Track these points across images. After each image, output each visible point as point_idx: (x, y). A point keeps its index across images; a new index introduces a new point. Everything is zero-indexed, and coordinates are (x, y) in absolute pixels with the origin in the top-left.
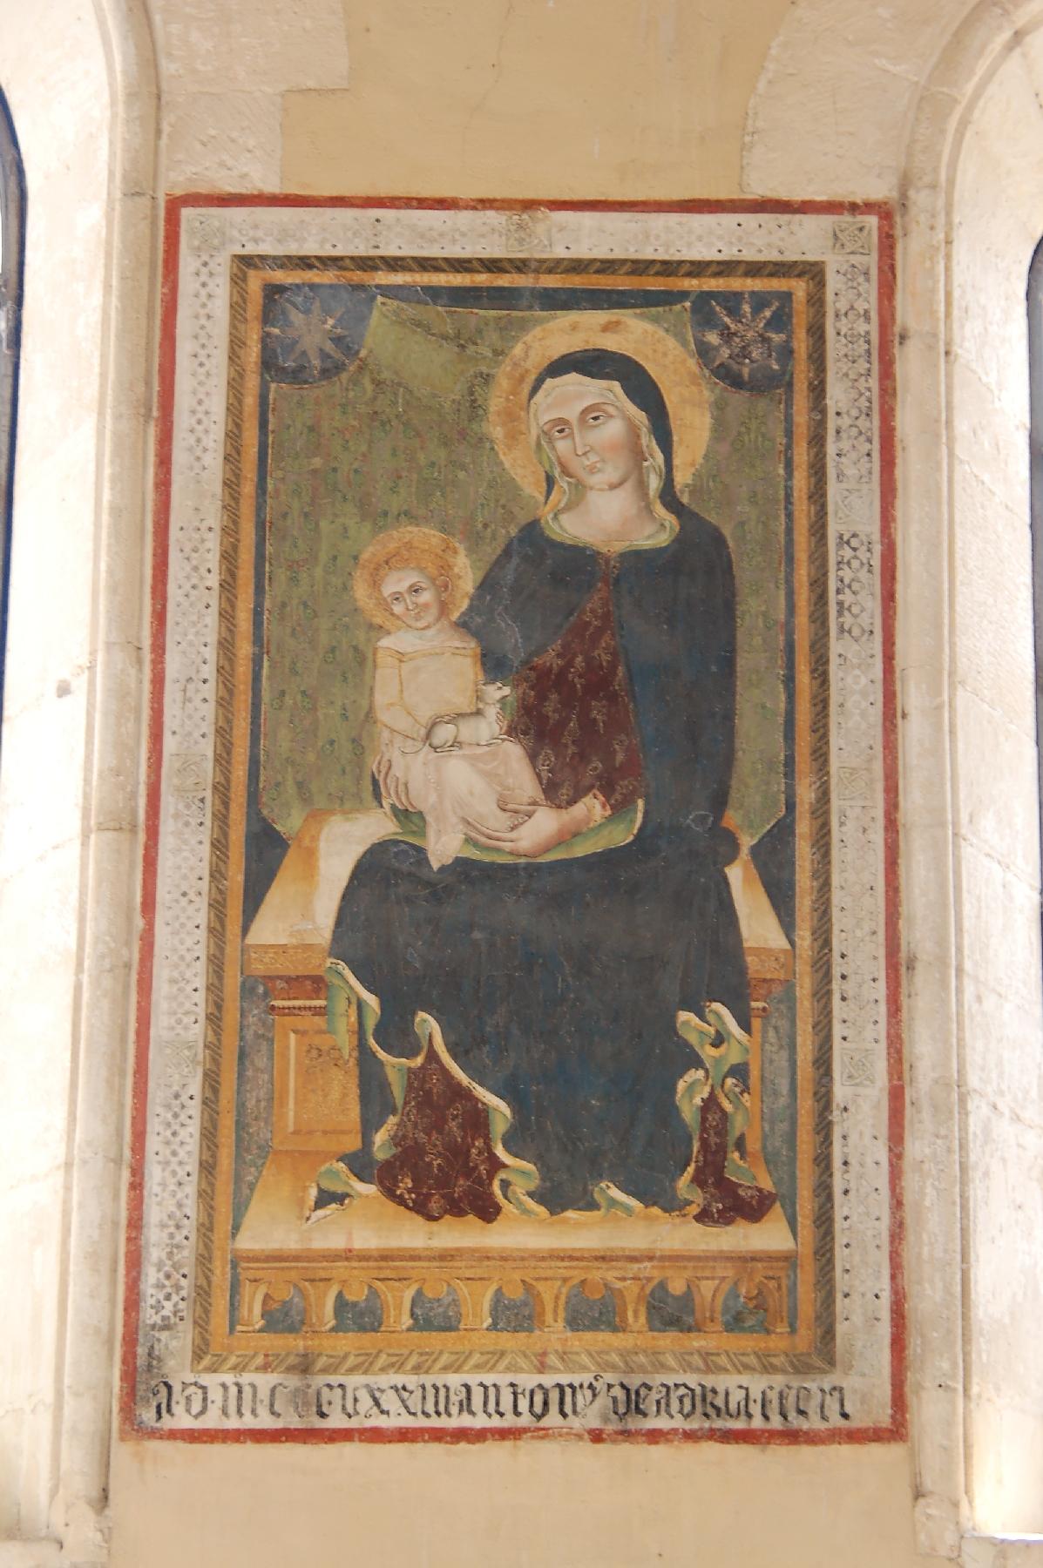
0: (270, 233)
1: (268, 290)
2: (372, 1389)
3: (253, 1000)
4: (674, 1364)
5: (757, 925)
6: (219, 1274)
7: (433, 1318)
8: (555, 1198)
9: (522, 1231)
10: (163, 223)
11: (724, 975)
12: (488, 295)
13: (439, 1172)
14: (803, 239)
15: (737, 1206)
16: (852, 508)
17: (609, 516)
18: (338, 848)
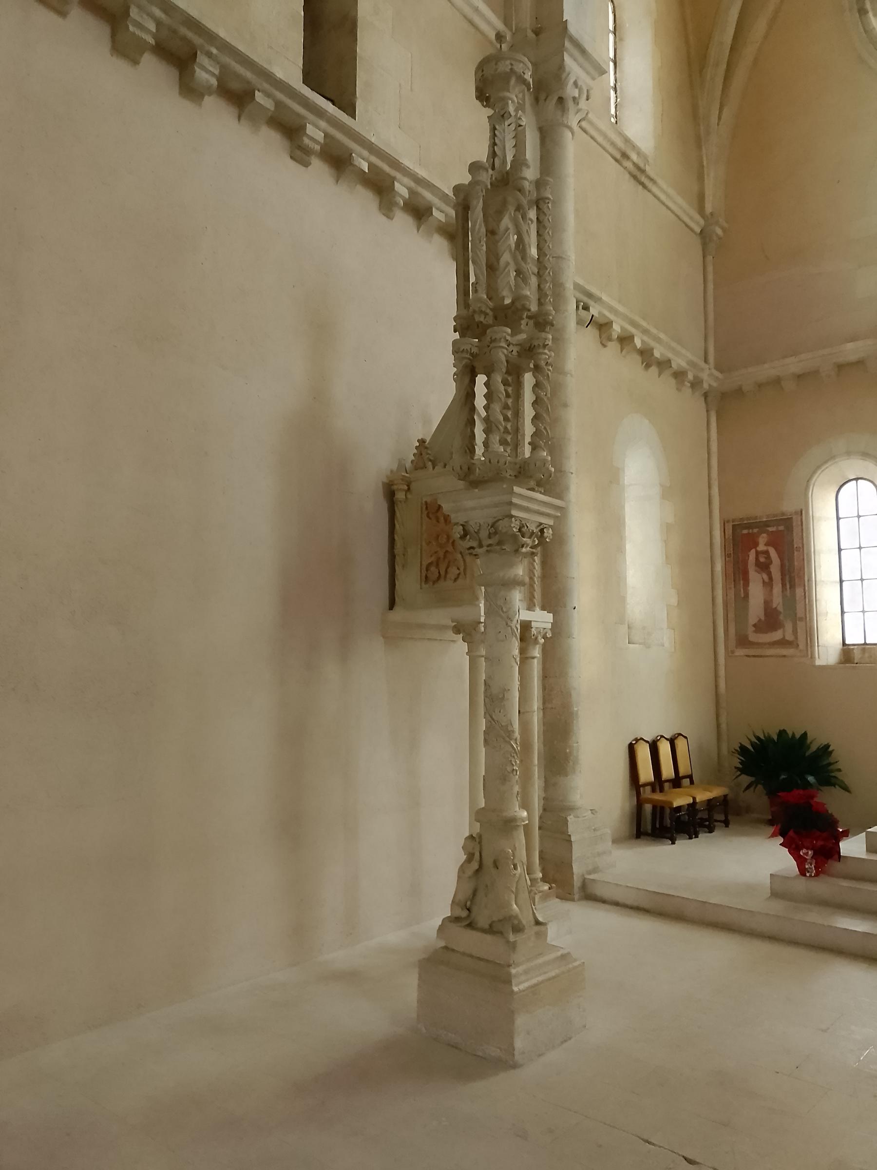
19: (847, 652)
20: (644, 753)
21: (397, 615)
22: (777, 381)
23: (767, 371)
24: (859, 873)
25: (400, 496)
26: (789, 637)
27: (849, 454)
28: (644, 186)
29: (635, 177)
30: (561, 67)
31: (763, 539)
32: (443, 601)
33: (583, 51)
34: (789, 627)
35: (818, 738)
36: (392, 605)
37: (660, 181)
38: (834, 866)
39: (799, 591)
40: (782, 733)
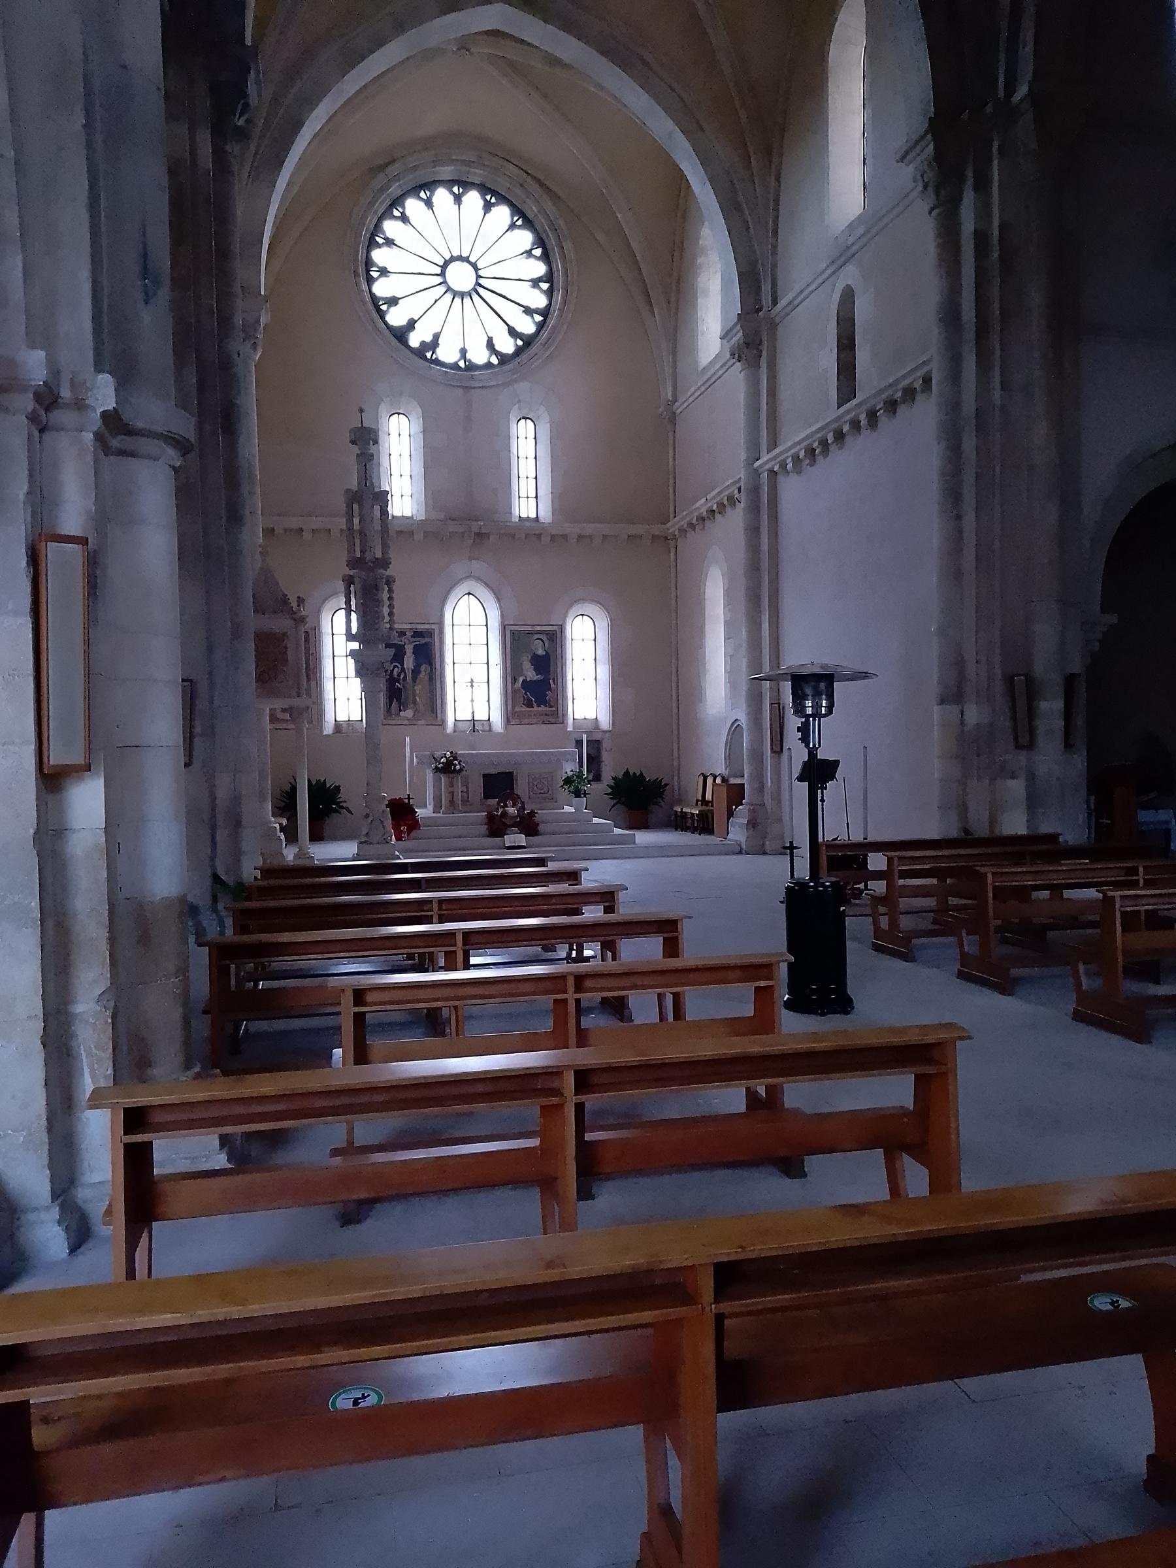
1: (513, 633)
3: (514, 691)
4: (546, 718)
5: (552, 685)
6: (513, 712)
7: (530, 715)
8: (539, 706)
10: (504, 627)
11: (550, 689)
12: (531, 633)
13: (530, 705)
14: (555, 628)
16: (559, 651)
17: (540, 652)
18: (521, 679)
19: (338, 726)
23: (294, 523)
38: (414, 834)
39: (313, 684)
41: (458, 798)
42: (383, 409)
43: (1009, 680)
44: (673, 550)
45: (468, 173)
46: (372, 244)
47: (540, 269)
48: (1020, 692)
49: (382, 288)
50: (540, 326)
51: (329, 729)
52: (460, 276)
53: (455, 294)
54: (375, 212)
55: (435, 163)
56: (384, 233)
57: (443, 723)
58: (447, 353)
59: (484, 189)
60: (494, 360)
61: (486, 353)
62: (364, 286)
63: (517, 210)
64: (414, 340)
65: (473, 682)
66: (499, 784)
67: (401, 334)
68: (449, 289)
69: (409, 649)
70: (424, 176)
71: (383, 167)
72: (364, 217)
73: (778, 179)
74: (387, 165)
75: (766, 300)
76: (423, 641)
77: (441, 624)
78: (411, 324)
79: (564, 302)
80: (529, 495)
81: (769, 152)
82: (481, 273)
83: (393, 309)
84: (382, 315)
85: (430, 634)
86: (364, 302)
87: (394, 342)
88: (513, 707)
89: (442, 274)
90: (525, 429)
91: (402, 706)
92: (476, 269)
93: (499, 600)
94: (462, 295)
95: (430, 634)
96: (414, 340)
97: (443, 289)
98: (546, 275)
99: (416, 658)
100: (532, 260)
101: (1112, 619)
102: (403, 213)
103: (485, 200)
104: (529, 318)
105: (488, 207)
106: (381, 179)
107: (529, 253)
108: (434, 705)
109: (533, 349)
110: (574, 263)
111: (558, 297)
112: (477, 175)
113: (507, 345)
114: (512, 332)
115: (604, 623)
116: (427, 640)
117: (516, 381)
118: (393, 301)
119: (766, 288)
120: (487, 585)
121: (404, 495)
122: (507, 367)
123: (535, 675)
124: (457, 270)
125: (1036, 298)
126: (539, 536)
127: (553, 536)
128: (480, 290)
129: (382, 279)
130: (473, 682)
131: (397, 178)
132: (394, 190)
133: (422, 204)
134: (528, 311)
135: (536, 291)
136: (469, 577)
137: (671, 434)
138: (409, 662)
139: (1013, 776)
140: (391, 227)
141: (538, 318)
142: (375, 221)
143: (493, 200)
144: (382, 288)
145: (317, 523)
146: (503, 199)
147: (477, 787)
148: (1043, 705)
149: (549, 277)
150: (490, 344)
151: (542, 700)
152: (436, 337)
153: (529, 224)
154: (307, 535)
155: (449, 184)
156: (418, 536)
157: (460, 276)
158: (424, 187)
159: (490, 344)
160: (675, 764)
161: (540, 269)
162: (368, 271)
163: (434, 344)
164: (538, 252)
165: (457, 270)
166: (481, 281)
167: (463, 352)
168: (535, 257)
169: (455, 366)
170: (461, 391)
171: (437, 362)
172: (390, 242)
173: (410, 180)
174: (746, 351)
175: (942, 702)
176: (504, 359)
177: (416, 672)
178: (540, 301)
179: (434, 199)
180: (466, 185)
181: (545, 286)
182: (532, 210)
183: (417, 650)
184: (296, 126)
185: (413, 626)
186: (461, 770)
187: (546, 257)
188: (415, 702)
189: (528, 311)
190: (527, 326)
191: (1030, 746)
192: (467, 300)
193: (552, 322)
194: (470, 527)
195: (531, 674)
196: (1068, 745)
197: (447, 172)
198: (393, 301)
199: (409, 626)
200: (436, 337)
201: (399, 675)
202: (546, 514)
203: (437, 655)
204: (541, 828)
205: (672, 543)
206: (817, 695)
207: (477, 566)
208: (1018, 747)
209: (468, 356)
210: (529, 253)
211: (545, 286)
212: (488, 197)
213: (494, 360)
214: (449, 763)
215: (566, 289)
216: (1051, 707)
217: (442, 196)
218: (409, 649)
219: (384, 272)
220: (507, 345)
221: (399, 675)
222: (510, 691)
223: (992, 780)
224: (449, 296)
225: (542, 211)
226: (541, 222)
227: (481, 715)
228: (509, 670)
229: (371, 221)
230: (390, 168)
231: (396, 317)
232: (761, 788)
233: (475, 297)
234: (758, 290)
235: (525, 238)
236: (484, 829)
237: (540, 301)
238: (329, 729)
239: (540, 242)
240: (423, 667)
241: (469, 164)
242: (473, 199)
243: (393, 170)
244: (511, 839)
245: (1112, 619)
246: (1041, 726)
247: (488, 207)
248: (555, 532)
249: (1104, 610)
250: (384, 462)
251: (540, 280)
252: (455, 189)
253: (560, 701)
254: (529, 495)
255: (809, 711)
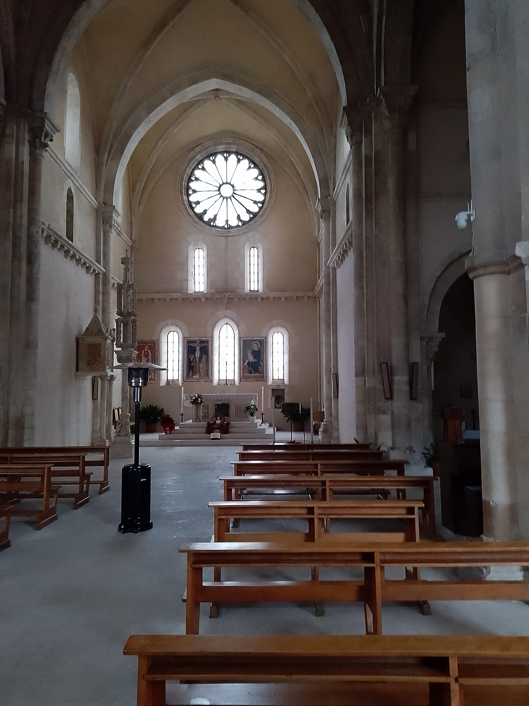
0: (243, 338)
1: (244, 341)
2: (248, 380)
3: (244, 367)
4: (258, 379)
6: (243, 377)
9: (253, 374)
12: (252, 341)
13: (250, 372)
15: (260, 373)
16: (265, 349)
17: (256, 349)
18: (247, 362)
20: (116, 411)
21: (79, 373)
22: (153, 299)
23: (151, 296)
24: (178, 432)
25: (80, 342)
26: (153, 378)
27: (172, 325)
28: (120, 236)
29: (118, 234)
30: (112, 216)
31: (146, 347)
32: (93, 370)
33: (117, 212)
34: (153, 374)
35: (160, 406)
36: (77, 370)
37: (124, 235)
38: (173, 431)
40: (150, 406)
41: (201, 414)
42: (190, 247)
43: (380, 365)
44: (318, 303)
45: (230, 148)
46: (190, 180)
47: (262, 184)
48: (387, 371)
49: (193, 198)
50: (261, 208)
51: (163, 383)
52: (227, 191)
53: (224, 198)
54: (191, 167)
55: (216, 145)
56: (195, 176)
57: (212, 381)
58: (220, 222)
59: (237, 154)
60: (240, 224)
61: (237, 221)
62: (185, 198)
63: (251, 161)
64: (206, 218)
65: (226, 362)
66: (223, 409)
67: (200, 217)
68: (221, 196)
69: (198, 348)
70: (211, 150)
71: (192, 149)
72: (185, 170)
73: (335, 137)
74: (195, 147)
75: (331, 191)
76: (204, 345)
77: (212, 337)
78: (205, 212)
79: (270, 198)
80: (254, 280)
81: (332, 127)
82: (235, 188)
83: (198, 206)
84: (193, 209)
85: (207, 342)
86: (184, 204)
87: (197, 220)
88: (243, 373)
89: (219, 190)
90: (254, 252)
91: (194, 373)
92: (220, 186)
93: (238, 327)
94: (227, 198)
95: (207, 342)
96: (206, 218)
97: (219, 196)
98: (263, 187)
99: (201, 353)
100: (258, 181)
101: (444, 335)
102: (203, 167)
103: (238, 158)
104: (255, 205)
105: (239, 161)
106: (192, 154)
107: (256, 179)
108: (208, 373)
109: (256, 218)
110: (275, 181)
111: (268, 195)
112: (234, 148)
113: (246, 217)
114: (248, 211)
115: (286, 336)
116: (206, 344)
117: (246, 232)
118: (198, 203)
119: (331, 186)
120: (233, 320)
121: (198, 282)
122: (246, 226)
123: (254, 360)
124: (227, 188)
125: (391, 183)
126: (256, 298)
127: (262, 298)
128: (235, 196)
129: (194, 194)
130: (226, 362)
131: (200, 152)
132: (199, 157)
133: (211, 162)
134: (255, 202)
135: (259, 194)
136: (226, 316)
137: (318, 251)
138: (197, 354)
139: (384, 413)
140: (198, 173)
141: (260, 205)
142: (191, 170)
143: (241, 158)
144: (193, 198)
145: (159, 296)
146: (245, 157)
147: (212, 412)
148: (396, 378)
149: (265, 188)
150: (239, 217)
151: (256, 371)
152: (215, 216)
153: (256, 166)
154: (156, 301)
155: (222, 153)
156: (203, 300)
157: (227, 191)
158: (211, 155)
159: (239, 217)
160: (319, 401)
161: (262, 184)
162: (188, 191)
163: (215, 219)
164: (260, 177)
165: (227, 188)
166: (236, 192)
167: (227, 221)
168: (259, 180)
169: (223, 228)
170: (224, 238)
171: (216, 227)
172: (197, 179)
173: (205, 153)
174: (324, 215)
175: (356, 375)
176: (244, 223)
177: (201, 358)
178: (261, 198)
179: (216, 160)
180: (230, 153)
181: (263, 191)
182: (257, 161)
183: (201, 349)
184: (128, 137)
185: (200, 339)
186: (202, 402)
187: (264, 180)
188: (200, 372)
189: (255, 202)
190: (255, 209)
191: (391, 398)
192: (229, 200)
193: (265, 206)
194: (226, 296)
195: (251, 359)
196: (413, 397)
197: (221, 148)
198: (198, 203)
199: (198, 339)
200: (215, 216)
201: (193, 360)
202: (261, 289)
203: (210, 351)
204: (231, 430)
205: (318, 300)
206: (137, 377)
207: (228, 312)
208: (387, 399)
209: (229, 223)
210: (256, 179)
211: (263, 191)
212: (239, 157)
213: (240, 224)
214: (196, 399)
215: (271, 192)
216: (401, 380)
217: (220, 158)
218: (198, 348)
219: (194, 191)
220: (246, 217)
221: (193, 360)
222: (242, 367)
223: (376, 415)
224: (222, 199)
225: (261, 160)
226: (261, 165)
227: (230, 377)
228: (242, 357)
229: (188, 171)
230: (196, 149)
231: (199, 210)
232: (331, 414)
233: (232, 198)
234: (328, 188)
235: (255, 172)
236: (204, 430)
237: (261, 198)
238: (163, 383)
239: (261, 173)
240: (204, 357)
241: (229, 144)
242: (233, 158)
243: (198, 149)
244: (212, 435)
245: (444, 335)
246: (395, 387)
247: (239, 161)
248: (264, 296)
249: (440, 331)
250: (191, 269)
251: (261, 189)
252: (225, 155)
253: (265, 371)
254: (254, 280)
255: (133, 385)
